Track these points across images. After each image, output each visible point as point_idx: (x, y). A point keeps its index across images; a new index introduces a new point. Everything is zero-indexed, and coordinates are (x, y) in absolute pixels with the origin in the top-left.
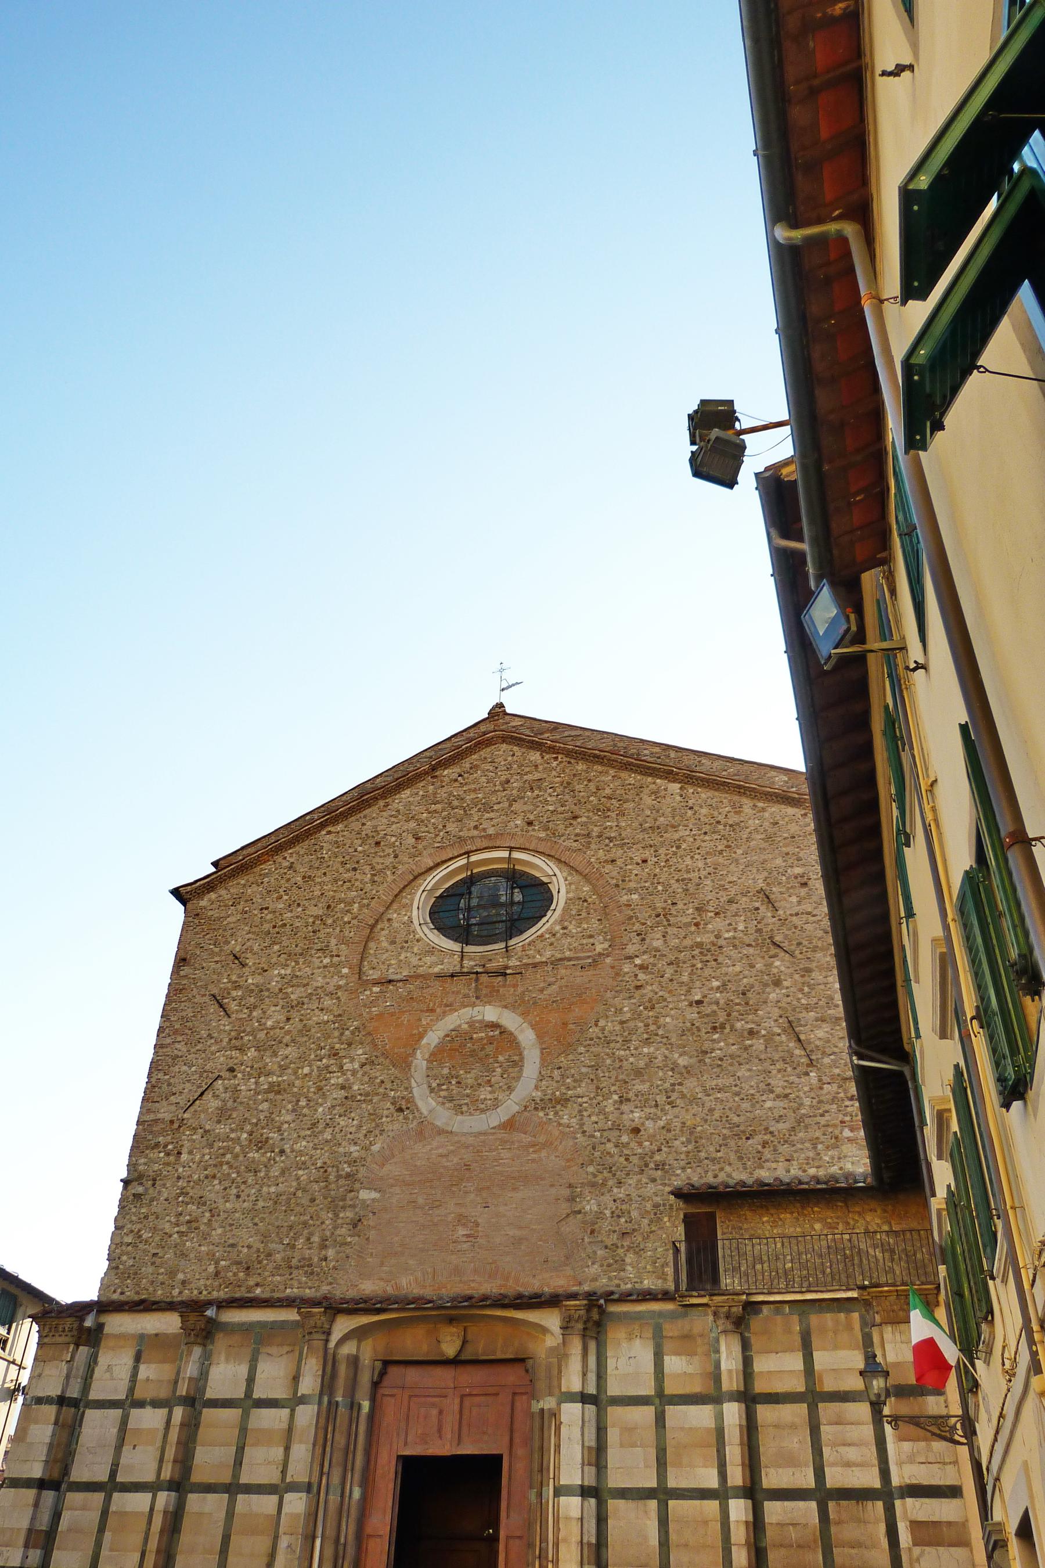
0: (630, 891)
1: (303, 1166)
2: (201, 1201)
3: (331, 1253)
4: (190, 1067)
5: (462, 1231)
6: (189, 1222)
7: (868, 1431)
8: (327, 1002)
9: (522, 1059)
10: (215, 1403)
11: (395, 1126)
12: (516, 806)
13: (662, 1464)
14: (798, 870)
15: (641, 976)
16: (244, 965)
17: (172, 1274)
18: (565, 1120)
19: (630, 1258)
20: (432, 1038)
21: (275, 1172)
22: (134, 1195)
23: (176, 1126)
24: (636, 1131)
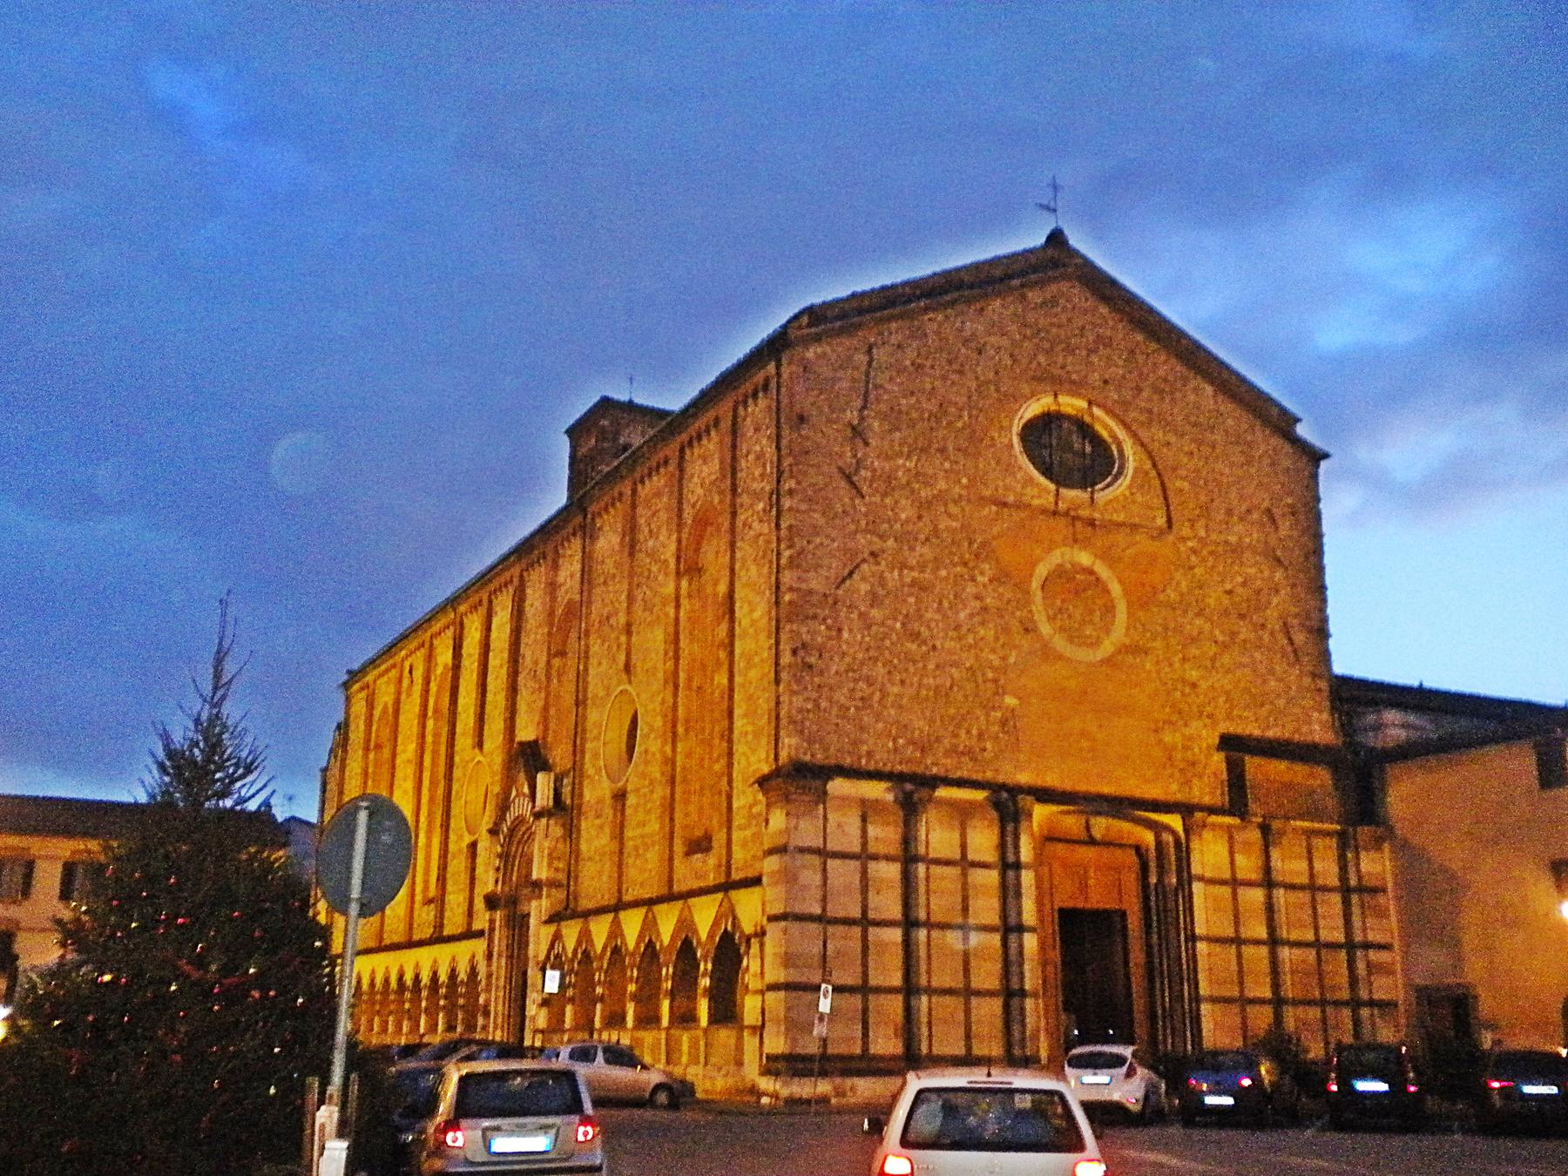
0: (1183, 478)
1: (955, 664)
2: (870, 682)
3: (989, 746)
4: (833, 540)
5: (1085, 744)
6: (862, 699)
8: (953, 509)
9: (1114, 607)
10: (938, 862)
11: (1026, 643)
12: (1094, 359)
13: (1237, 923)
14: (1289, 501)
15: (1193, 558)
16: (866, 444)
17: (855, 743)
18: (1148, 666)
19: (1195, 781)
20: (1042, 570)
21: (931, 666)
23: (830, 600)
24: (1194, 685)
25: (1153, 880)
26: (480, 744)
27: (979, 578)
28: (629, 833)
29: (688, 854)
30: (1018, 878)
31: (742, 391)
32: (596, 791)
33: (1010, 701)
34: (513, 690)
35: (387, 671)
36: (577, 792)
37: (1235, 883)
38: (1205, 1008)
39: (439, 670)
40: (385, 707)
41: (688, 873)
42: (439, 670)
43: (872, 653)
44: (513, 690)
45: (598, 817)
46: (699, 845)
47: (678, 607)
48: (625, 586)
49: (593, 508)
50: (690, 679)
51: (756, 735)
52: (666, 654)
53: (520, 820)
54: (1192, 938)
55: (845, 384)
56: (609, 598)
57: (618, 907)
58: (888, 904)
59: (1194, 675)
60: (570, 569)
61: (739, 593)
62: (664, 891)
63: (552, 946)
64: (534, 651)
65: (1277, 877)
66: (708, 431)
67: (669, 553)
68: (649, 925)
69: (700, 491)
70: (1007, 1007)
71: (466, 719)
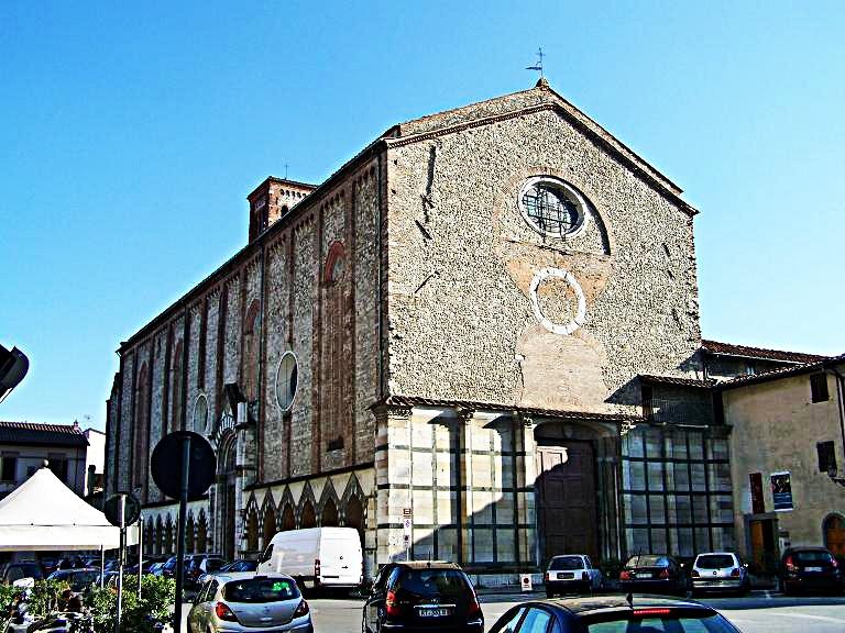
3: (505, 384)
5: (562, 381)
7: (703, 474)
10: (478, 453)
16: (432, 207)
20: (535, 281)
22: (397, 337)
25: (600, 459)
26: (201, 385)
27: (500, 286)
28: (294, 438)
29: (330, 449)
30: (523, 460)
31: (357, 175)
32: (274, 413)
33: (519, 357)
34: (221, 354)
35: (144, 343)
36: (262, 415)
37: (646, 460)
38: (628, 531)
39: (177, 342)
40: (144, 365)
41: (328, 460)
42: (177, 342)
43: (438, 331)
44: (221, 354)
45: (275, 428)
46: (337, 444)
47: (320, 304)
48: (288, 292)
49: (269, 245)
50: (328, 347)
51: (370, 380)
52: (314, 331)
53: (228, 431)
54: (622, 492)
55: (418, 171)
56: (279, 296)
57: (289, 480)
58: (445, 479)
59: (624, 341)
60: (255, 281)
61: (358, 295)
62: (315, 472)
63: (249, 505)
64: (233, 330)
65: (669, 455)
66: (337, 199)
67: (315, 272)
68: (307, 493)
69: (333, 235)
70: (516, 535)
71: (194, 371)
